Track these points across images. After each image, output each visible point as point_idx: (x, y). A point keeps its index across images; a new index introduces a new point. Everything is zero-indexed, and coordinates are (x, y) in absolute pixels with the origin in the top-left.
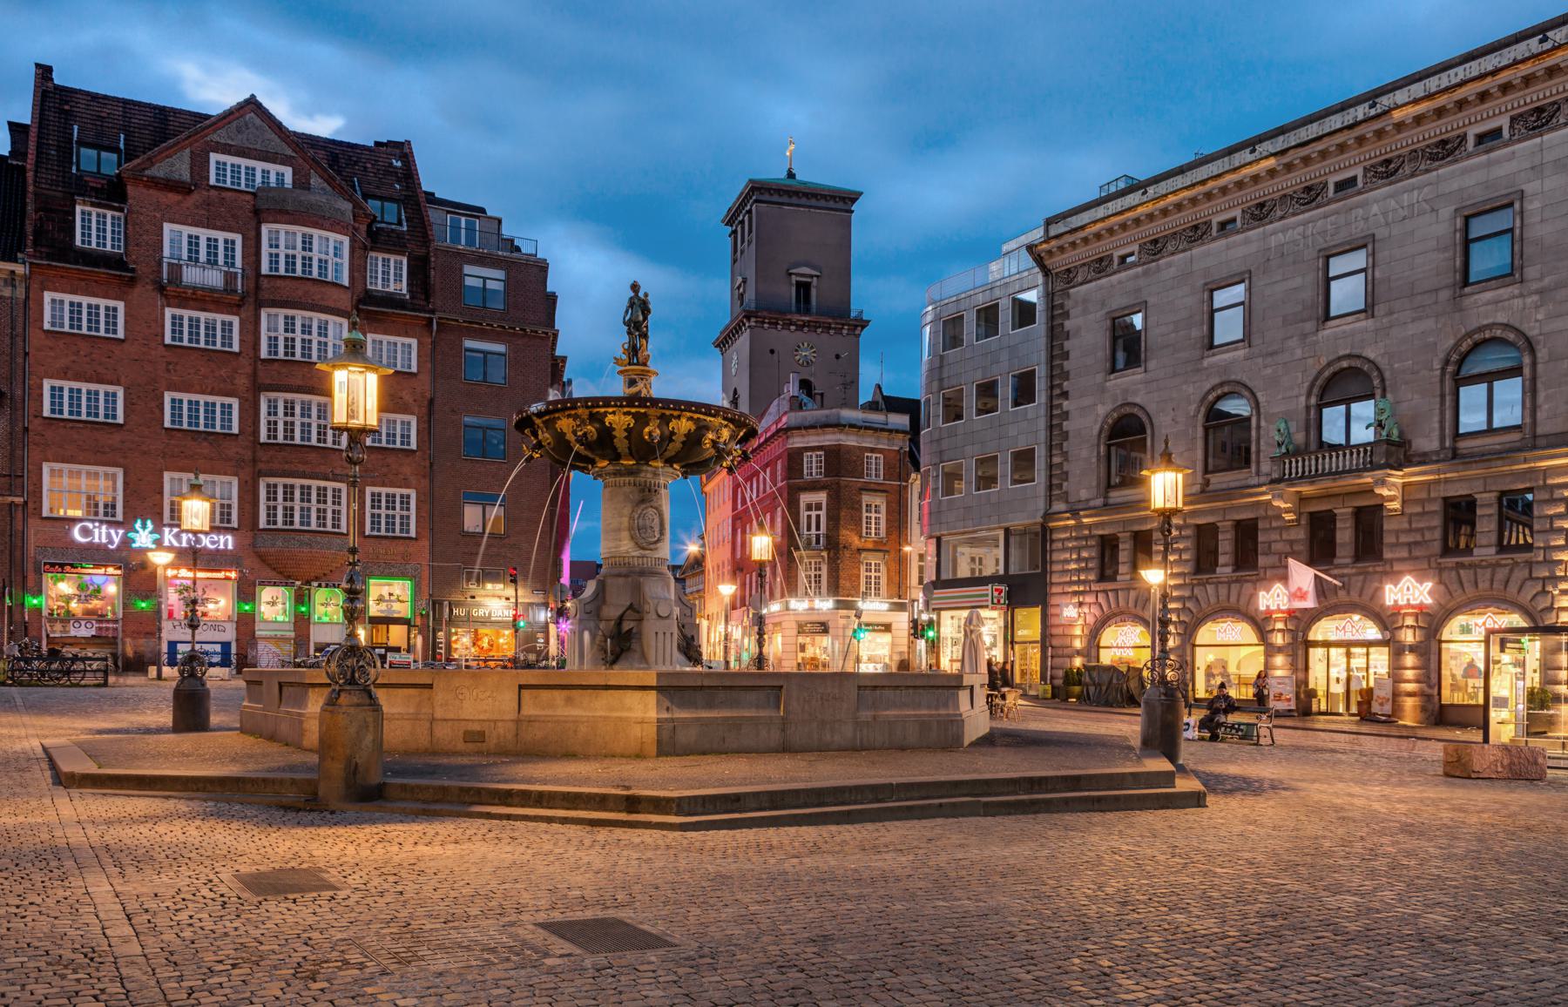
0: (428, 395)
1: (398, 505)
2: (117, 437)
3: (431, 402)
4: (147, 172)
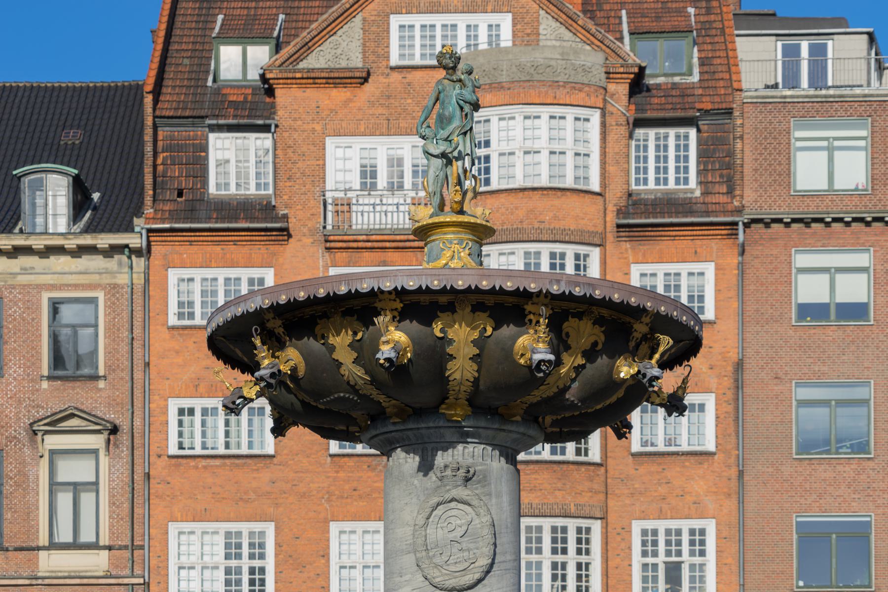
0: (734, 356)
1: (685, 548)
2: (264, 476)
3: (739, 366)
4: (302, 65)
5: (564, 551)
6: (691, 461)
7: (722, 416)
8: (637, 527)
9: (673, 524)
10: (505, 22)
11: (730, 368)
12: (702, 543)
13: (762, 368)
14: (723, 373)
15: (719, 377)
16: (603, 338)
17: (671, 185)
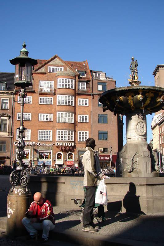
0: (91, 110)
1: (85, 135)
3: (91, 112)
5: (69, 135)
6: (85, 123)
8: (79, 132)
9: (83, 132)
10: (63, 68)
11: (90, 112)
12: (87, 134)
17: (83, 89)
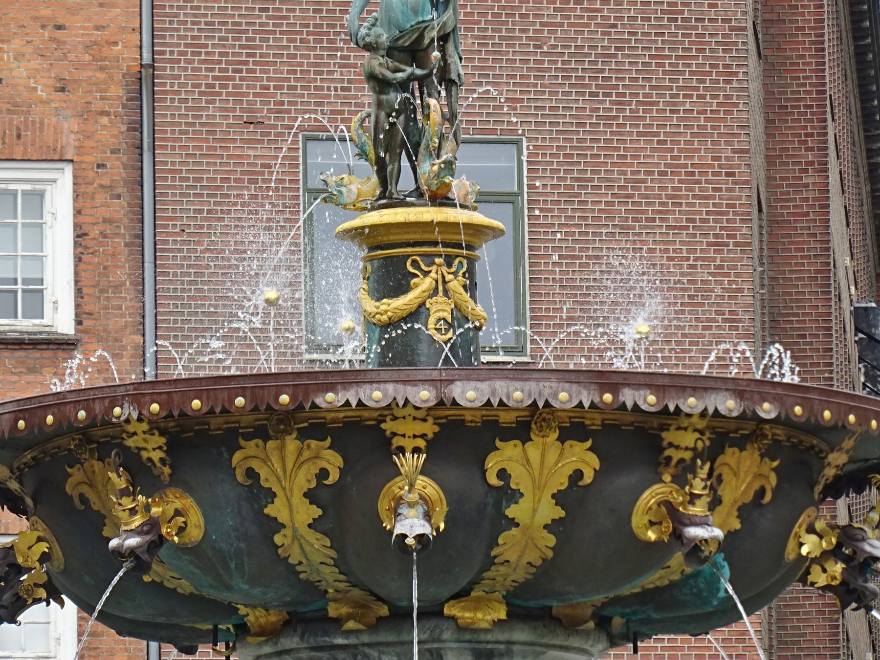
0: (126, 55)
3: (144, 82)
7: (95, 232)
11: (117, 91)
13: (210, 92)
14: (98, 105)
15: (86, 113)
16: (773, 479)
